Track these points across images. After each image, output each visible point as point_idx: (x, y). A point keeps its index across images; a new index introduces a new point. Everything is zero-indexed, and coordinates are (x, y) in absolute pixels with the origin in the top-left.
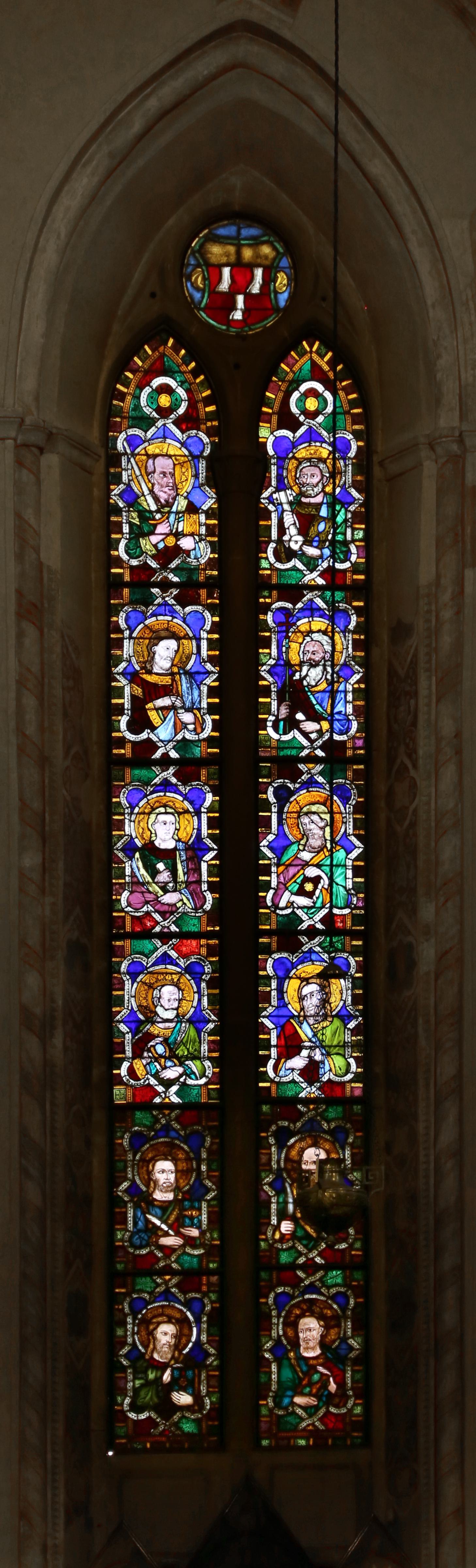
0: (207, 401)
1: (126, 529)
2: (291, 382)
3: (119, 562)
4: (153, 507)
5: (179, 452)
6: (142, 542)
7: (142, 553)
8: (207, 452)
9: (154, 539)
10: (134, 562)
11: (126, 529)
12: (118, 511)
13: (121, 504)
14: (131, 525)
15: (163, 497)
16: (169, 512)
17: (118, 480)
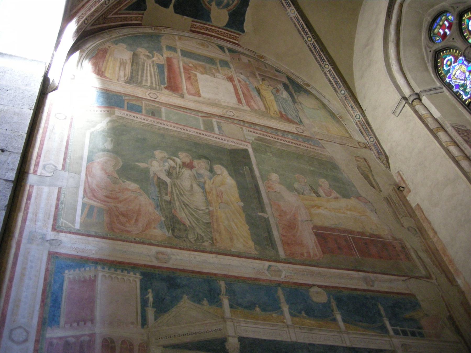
0: (456, 52)
1: (462, 93)
2: (467, 27)
3: (466, 100)
4: (462, 82)
5: (459, 67)
6: (467, 91)
7: (468, 92)
8: (463, 59)
9: (468, 87)
10: (469, 96)
11: (462, 93)
12: (458, 92)
13: (457, 90)
14: (462, 91)
15: (463, 78)
16: (467, 78)
17: (453, 86)
